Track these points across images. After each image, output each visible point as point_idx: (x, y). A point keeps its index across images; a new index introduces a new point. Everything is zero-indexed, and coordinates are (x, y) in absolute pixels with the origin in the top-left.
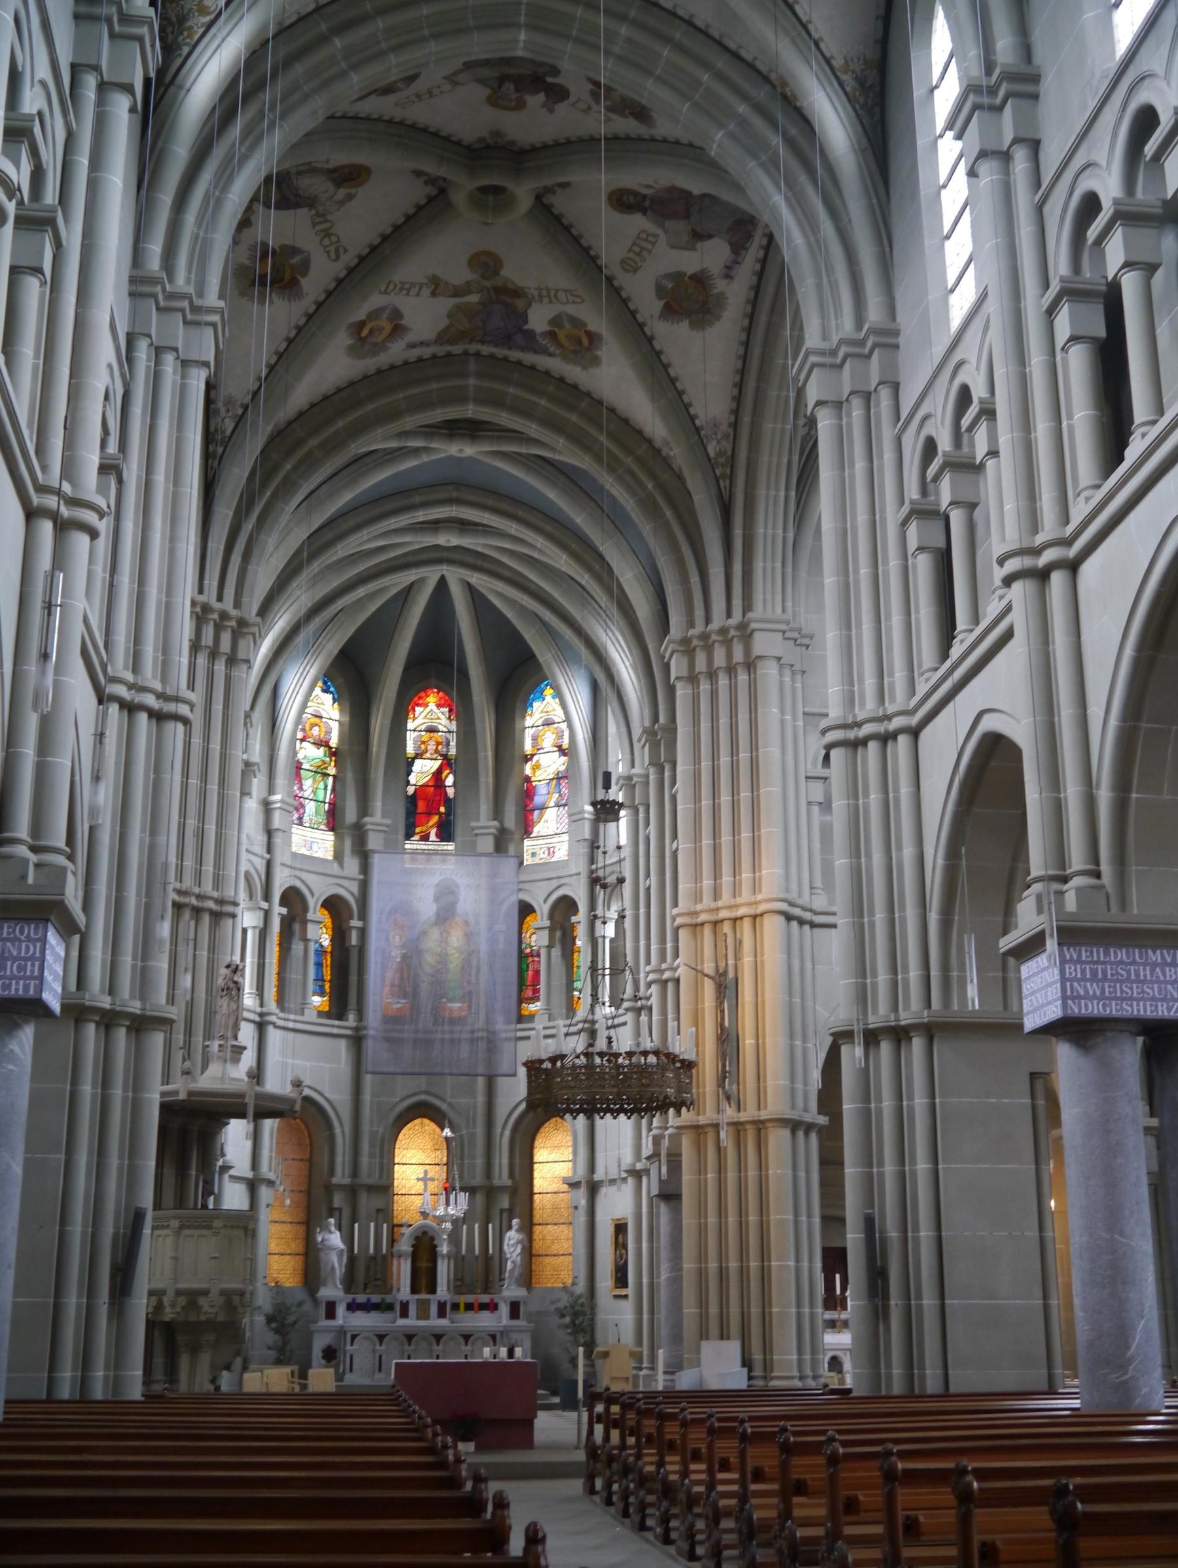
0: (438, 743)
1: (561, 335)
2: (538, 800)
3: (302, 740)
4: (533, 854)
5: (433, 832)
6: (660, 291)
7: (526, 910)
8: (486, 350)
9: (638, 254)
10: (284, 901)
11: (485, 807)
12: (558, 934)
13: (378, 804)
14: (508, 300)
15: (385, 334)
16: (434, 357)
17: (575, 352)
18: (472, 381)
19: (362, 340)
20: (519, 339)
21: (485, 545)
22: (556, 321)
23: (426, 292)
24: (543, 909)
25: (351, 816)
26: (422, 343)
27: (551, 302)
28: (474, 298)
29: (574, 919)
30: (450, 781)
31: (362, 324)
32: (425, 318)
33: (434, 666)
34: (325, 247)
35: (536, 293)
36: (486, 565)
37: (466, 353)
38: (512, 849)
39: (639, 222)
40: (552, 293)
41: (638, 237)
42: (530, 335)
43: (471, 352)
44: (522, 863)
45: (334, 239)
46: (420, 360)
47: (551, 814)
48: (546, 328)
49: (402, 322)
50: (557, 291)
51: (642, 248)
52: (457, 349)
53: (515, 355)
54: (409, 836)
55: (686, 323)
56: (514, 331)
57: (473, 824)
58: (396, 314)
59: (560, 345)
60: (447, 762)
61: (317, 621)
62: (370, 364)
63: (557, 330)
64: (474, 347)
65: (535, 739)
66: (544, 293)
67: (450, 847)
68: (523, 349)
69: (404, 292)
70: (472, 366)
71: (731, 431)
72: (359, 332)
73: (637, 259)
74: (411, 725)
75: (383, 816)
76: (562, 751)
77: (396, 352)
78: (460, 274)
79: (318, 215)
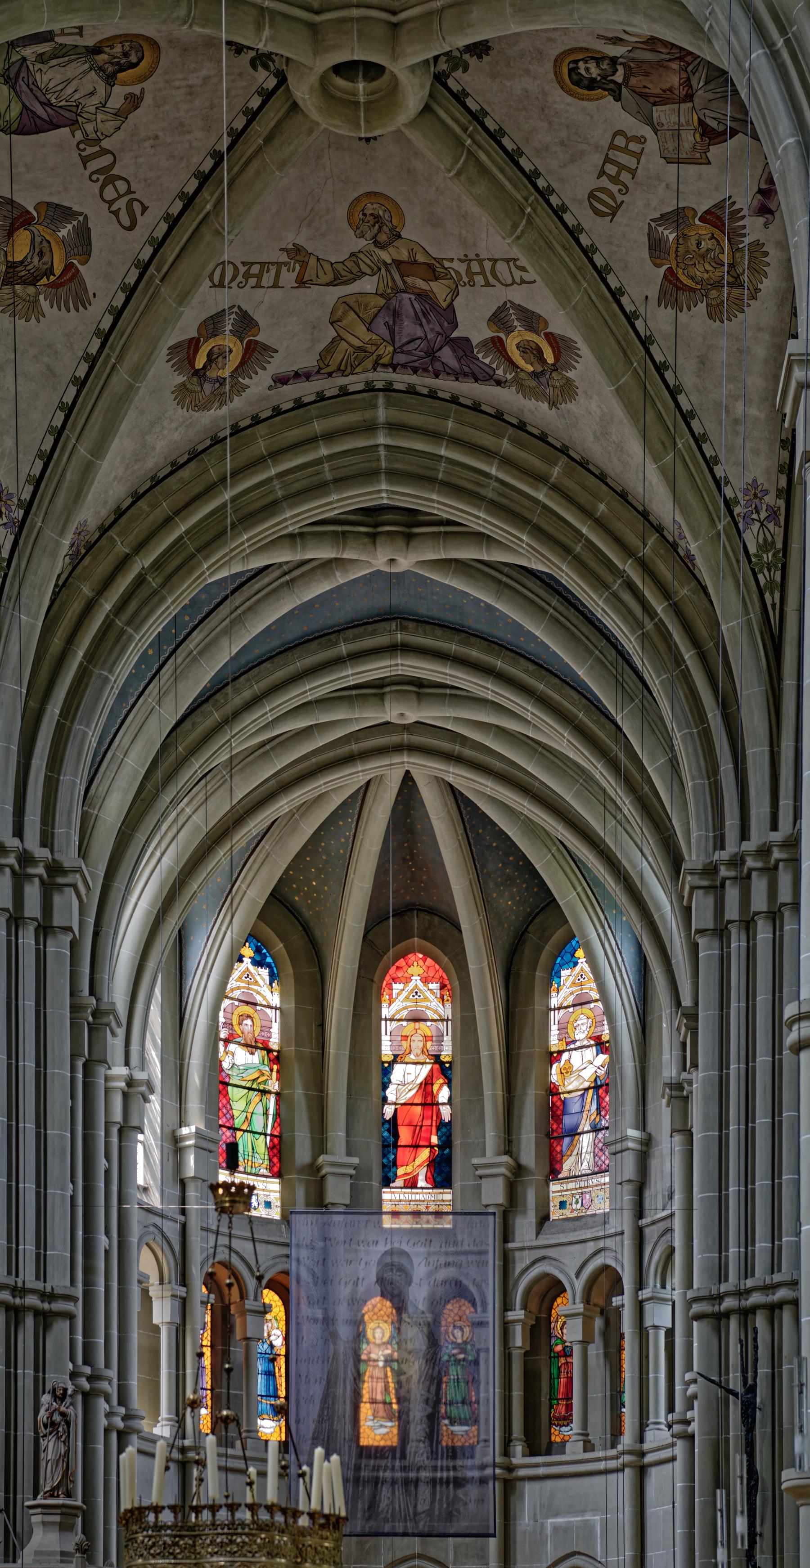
8: (402, 380)
15: (235, 359)
16: (321, 397)
18: (382, 439)
19: (200, 375)
20: (447, 355)
22: (499, 319)
26: (297, 375)
27: (488, 284)
28: (368, 285)
31: (193, 345)
35: (462, 268)
40: (488, 265)
43: (379, 385)
46: (299, 404)
50: (495, 261)
52: (355, 382)
53: (447, 386)
58: (246, 323)
59: (513, 365)
63: (502, 335)
64: (381, 377)
68: (458, 375)
69: (253, 281)
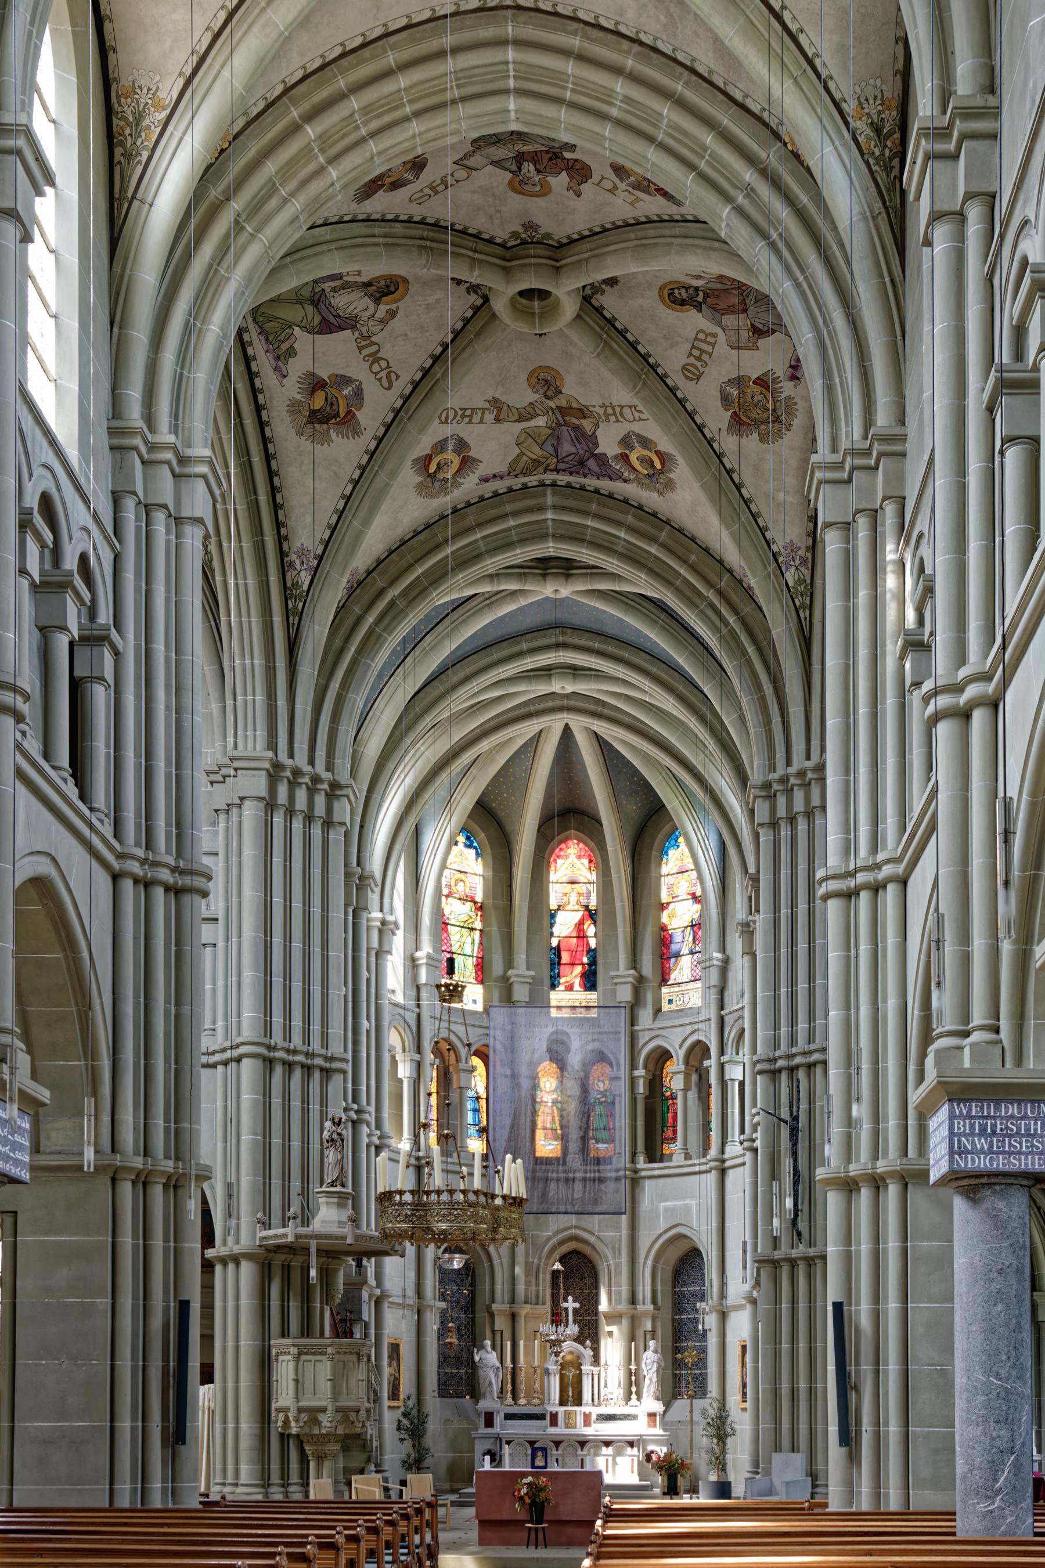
0: (580, 895)
1: (633, 457)
2: (674, 948)
3: (447, 896)
4: (670, 1002)
5: (577, 981)
7: (663, 1056)
8: (562, 479)
10: (437, 1051)
11: (623, 958)
12: (694, 1078)
13: (520, 957)
14: (575, 421)
16: (510, 490)
17: (648, 476)
19: (432, 476)
20: (592, 464)
21: (599, 691)
22: (626, 441)
23: (489, 417)
24: (679, 1054)
25: (497, 967)
26: (495, 476)
27: (617, 421)
28: (541, 421)
29: (706, 1063)
30: (590, 930)
31: (428, 458)
32: (494, 447)
33: (568, 816)
35: (601, 411)
36: (606, 711)
37: (542, 484)
38: (649, 997)
40: (618, 409)
42: (602, 460)
43: (548, 482)
44: (658, 1010)
46: (496, 495)
47: (686, 961)
48: (618, 451)
49: (471, 454)
52: (532, 480)
53: (591, 482)
54: (553, 986)
56: (588, 459)
57: (612, 973)
58: (462, 445)
60: (591, 914)
61: (444, 777)
62: (443, 502)
64: (549, 477)
65: (670, 888)
66: (610, 411)
67: (593, 996)
69: (467, 420)
70: (550, 500)
72: (427, 469)
74: (553, 877)
75: (528, 969)
76: (695, 898)
77: (469, 487)
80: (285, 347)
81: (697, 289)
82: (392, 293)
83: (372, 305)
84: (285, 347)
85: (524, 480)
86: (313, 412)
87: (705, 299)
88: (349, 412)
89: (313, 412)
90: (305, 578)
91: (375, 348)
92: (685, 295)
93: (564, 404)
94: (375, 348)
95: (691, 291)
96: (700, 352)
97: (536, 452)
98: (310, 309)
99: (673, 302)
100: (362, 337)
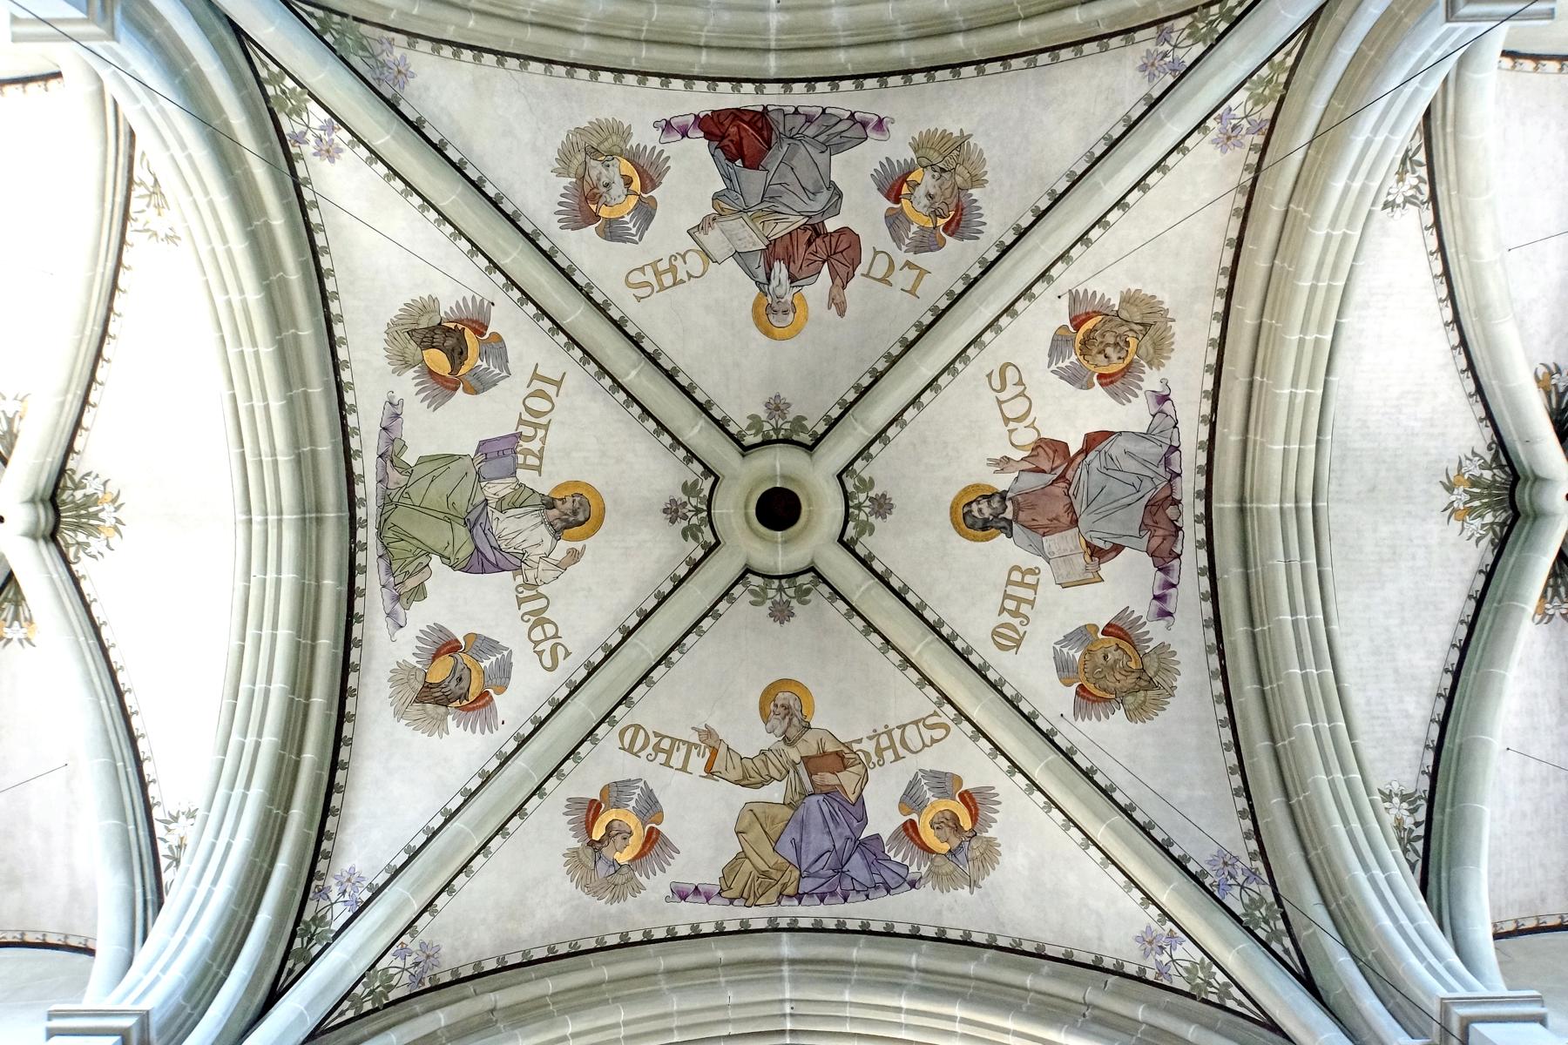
1: (928, 836)
6: (1064, 669)
9: (1015, 613)
14: (830, 779)
22: (911, 800)
23: (698, 763)
28: (775, 792)
31: (593, 809)
34: (537, 643)
35: (869, 746)
39: (1005, 551)
41: (1009, 582)
42: (871, 848)
45: (550, 629)
51: (1020, 600)
53: (856, 911)
55: (1120, 713)
58: (650, 807)
63: (914, 817)
69: (662, 757)
71: (1259, 864)
72: (589, 832)
73: (1015, 622)
78: (751, 736)
79: (526, 585)
80: (412, 583)
81: (1003, 496)
82: (580, 524)
83: (548, 539)
84: (412, 583)
85: (746, 913)
86: (428, 686)
87: (1016, 514)
88: (484, 694)
89: (428, 686)
90: (340, 914)
91: (541, 603)
92: (987, 512)
93: (813, 751)
94: (541, 603)
95: (996, 503)
96: (1017, 601)
97: (765, 857)
98: (462, 532)
99: (971, 527)
100: (526, 585)
